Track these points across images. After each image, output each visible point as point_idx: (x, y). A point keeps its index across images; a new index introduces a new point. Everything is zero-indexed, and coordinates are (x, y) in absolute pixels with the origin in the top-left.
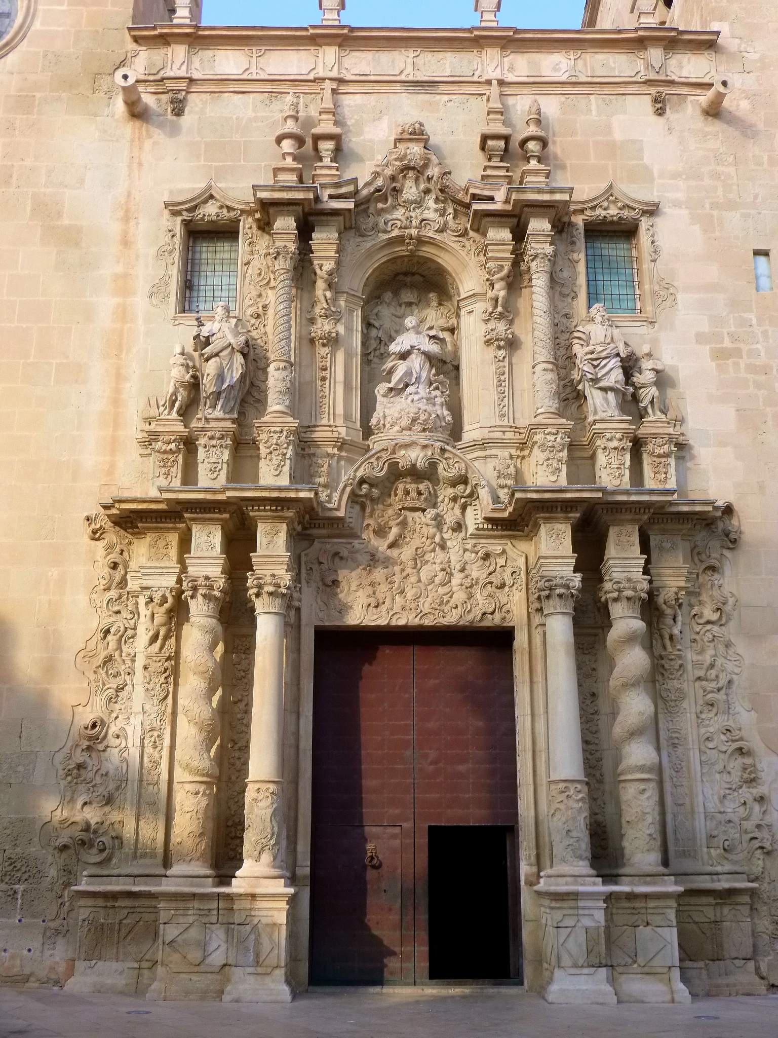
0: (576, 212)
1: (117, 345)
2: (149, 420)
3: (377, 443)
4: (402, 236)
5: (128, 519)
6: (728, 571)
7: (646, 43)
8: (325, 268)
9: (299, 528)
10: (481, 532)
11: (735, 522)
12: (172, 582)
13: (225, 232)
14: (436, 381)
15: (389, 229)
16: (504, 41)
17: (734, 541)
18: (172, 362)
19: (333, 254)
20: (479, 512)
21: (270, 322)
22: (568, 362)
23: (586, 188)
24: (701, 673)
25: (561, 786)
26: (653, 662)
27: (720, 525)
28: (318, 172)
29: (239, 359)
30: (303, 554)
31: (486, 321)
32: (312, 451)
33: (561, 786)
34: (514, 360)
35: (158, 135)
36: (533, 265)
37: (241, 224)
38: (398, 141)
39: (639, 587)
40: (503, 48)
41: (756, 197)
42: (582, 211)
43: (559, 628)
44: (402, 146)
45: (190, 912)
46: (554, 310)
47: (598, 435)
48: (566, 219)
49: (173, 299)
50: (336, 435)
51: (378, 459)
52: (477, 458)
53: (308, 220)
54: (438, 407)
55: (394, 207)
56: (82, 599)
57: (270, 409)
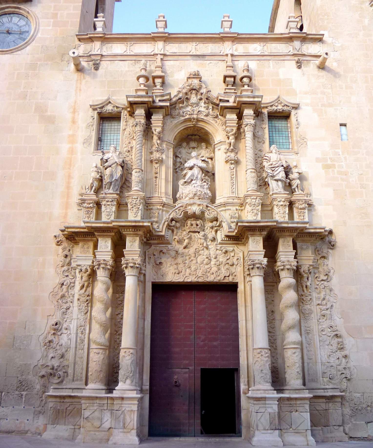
0: (264, 108)
1: (69, 164)
2: (82, 195)
3: (178, 204)
4: (190, 118)
6: (330, 258)
7: (293, 39)
8: (157, 131)
9: (145, 240)
10: (224, 242)
11: (333, 237)
12: (90, 263)
13: (115, 117)
14: (204, 179)
15: (185, 115)
16: (234, 39)
17: (333, 246)
18: (91, 170)
19: (160, 125)
20: (223, 233)
21: (133, 154)
22: (261, 170)
24: (319, 302)
25: (259, 350)
26: (299, 297)
27: (327, 239)
28: (154, 91)
29: (120, 168)
30: (147, 252)
31: (226, 153)
32: (151, 207)
33: (259, 350)
34: (238, 169)
35: (88, 78)
36: (246, 129)
37: (122, 114)
39: (292, 264)
40: (233, 41)
41: (340, 102)
42: (267, 107)
43: (258, 282)
44: (190, 81)
45: (95, 405)
46: (255, 147)
47: (274, 199)
48: (260, 110)
49: (93, 145)
50: (161, 201)
51: (179, 210)
52: (222, 210)
53: (150, 110)
54: (205, 190)
55: (187, 106)
56: (52, 271)
57: (133, 189)
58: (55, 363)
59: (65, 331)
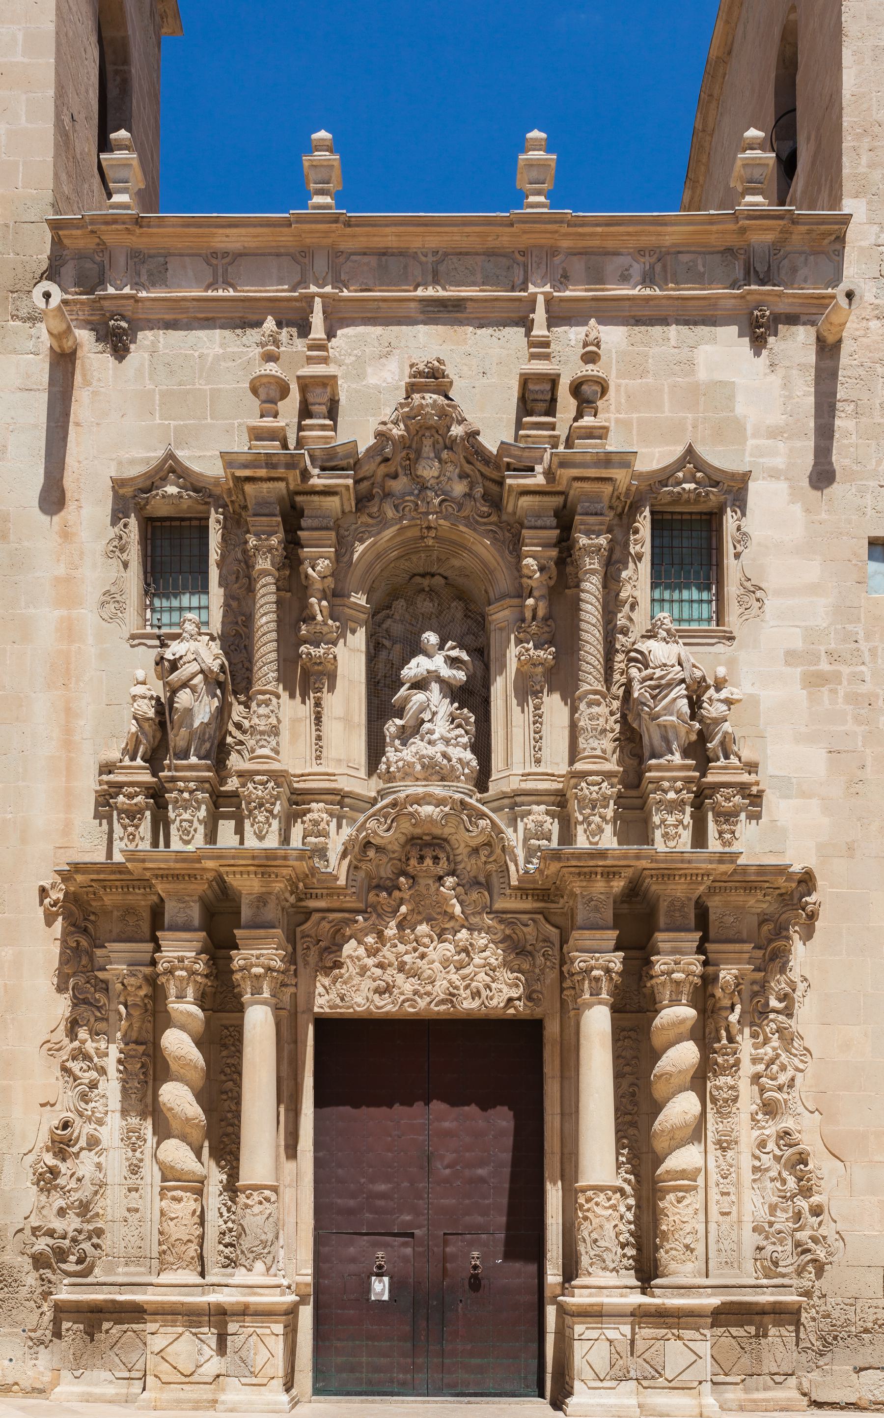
2: (107, 768)
5: (91, 889)
23: (657, 451)
38: (412, 389)
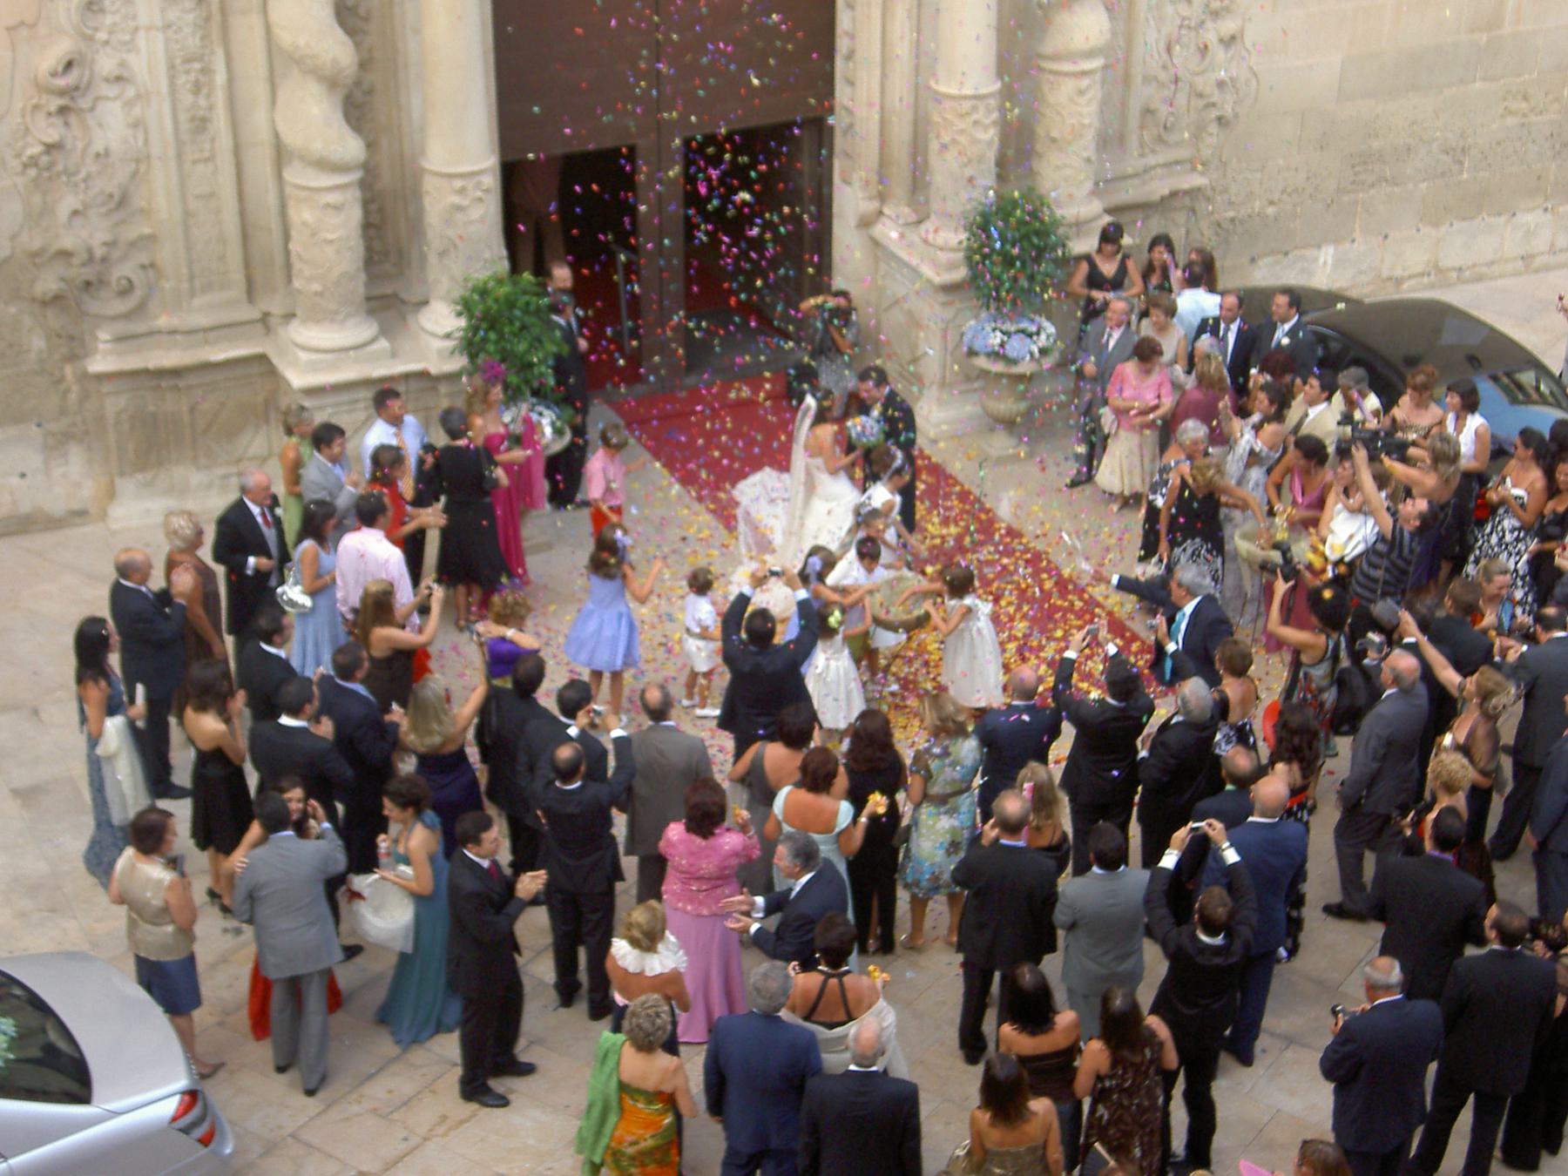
58: (94, 234)
59: (111, 91)
